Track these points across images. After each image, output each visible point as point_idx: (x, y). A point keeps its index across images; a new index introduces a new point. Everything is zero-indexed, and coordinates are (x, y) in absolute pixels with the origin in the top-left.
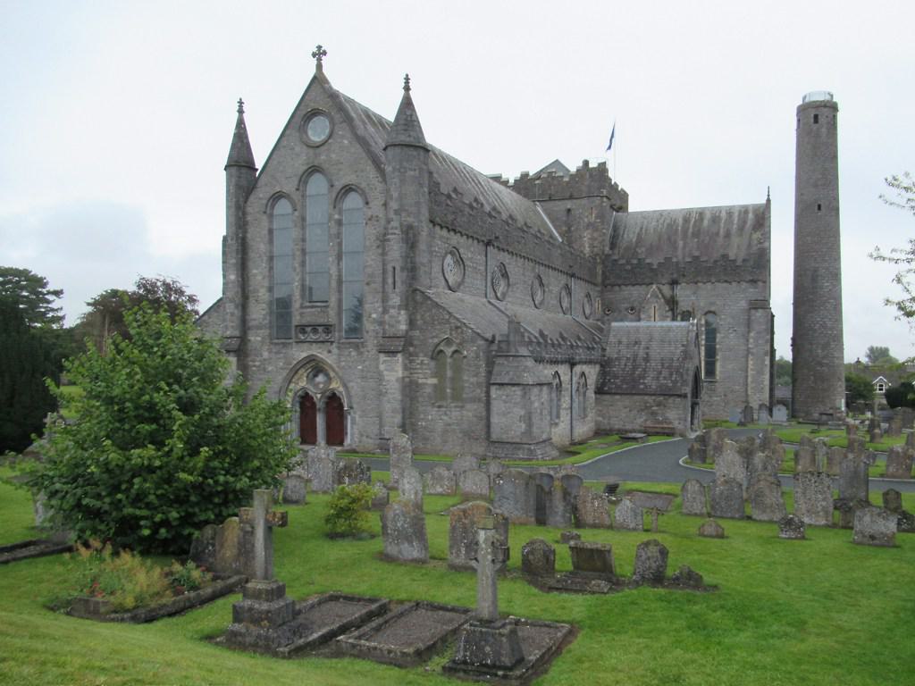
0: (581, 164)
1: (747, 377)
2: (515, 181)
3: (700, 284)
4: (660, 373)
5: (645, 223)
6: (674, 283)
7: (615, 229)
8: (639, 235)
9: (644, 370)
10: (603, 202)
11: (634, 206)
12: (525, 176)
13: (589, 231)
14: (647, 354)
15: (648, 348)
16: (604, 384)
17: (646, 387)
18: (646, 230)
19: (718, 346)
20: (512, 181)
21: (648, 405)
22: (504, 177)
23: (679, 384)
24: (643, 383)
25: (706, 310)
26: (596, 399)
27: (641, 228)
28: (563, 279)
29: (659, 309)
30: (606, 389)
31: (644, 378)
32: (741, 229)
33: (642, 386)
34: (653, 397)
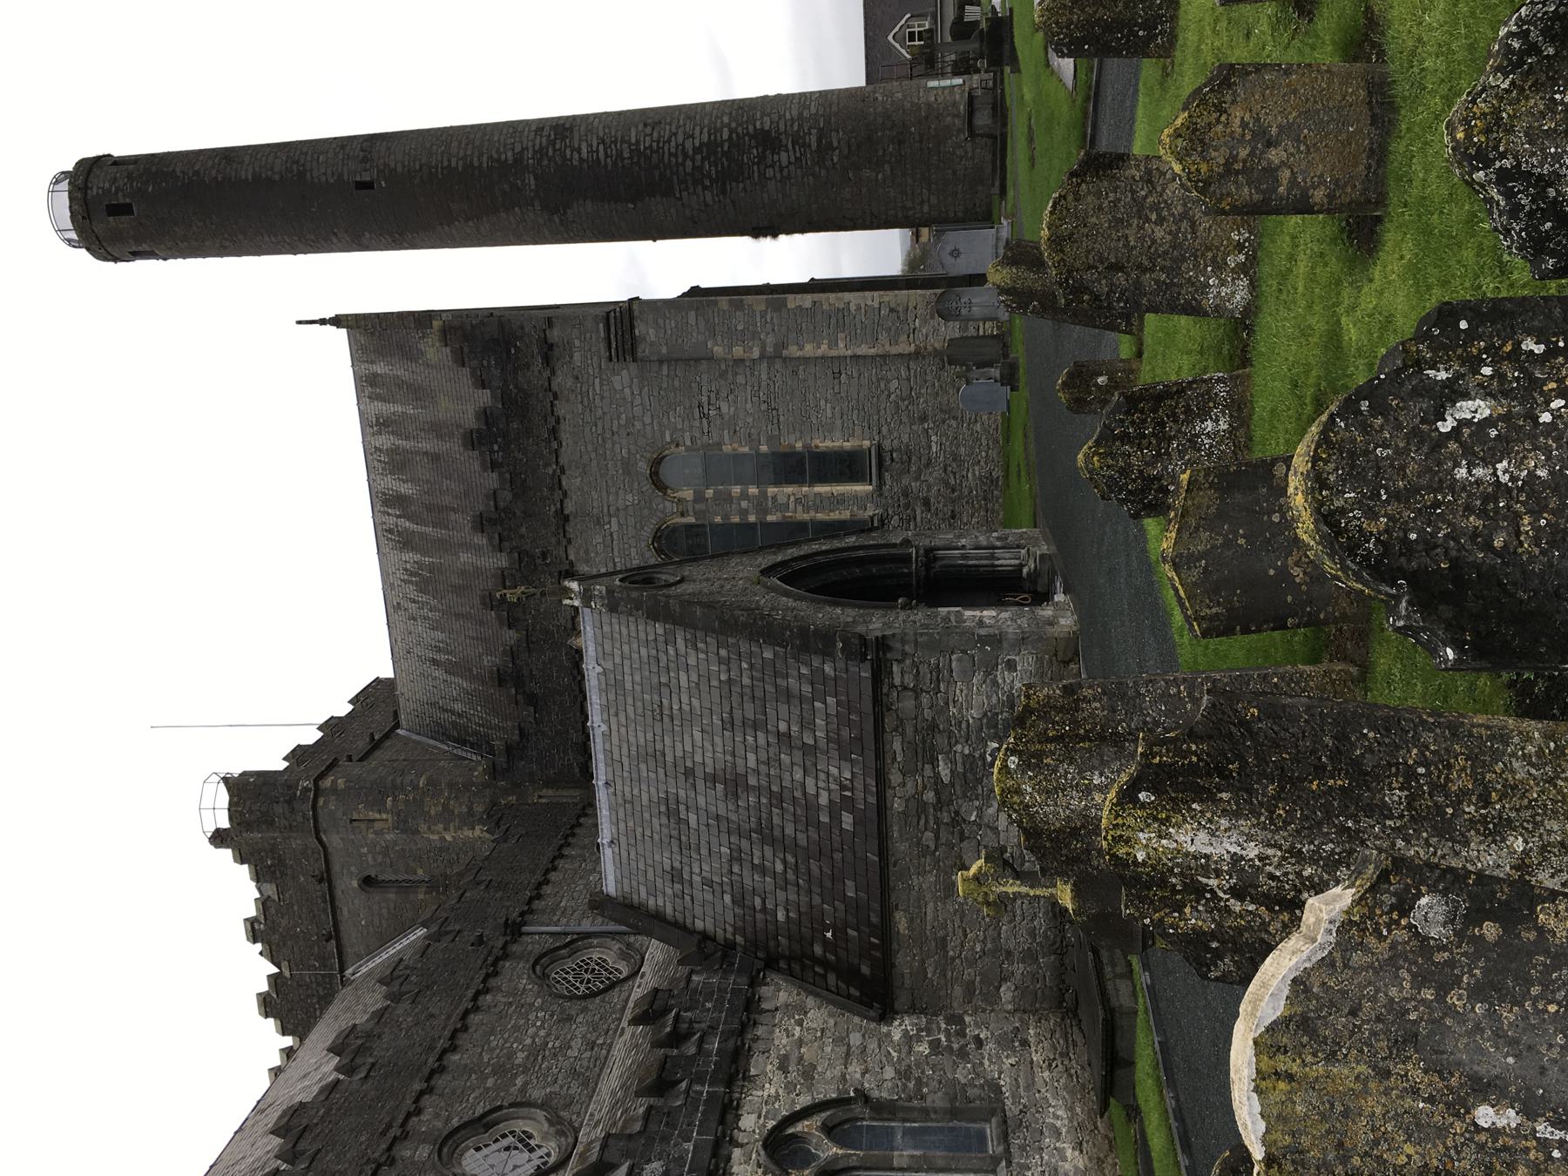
0: (227, 854)
2: (284, 1032)
3: (570, 507)
4: (784, 739)
5: (417, 650)
7: (441, 732)
8: (451, 669)
9: (778, 799)
10: (334, 789)
11: (387, 672)
12: (268, 1005)
13: (423, 827)
14: (712, 779)
15: (689, 773)
16: (849, 974)
17: (848, 804)
18: (439, 650)
19: (764, 448)
20: (288, 1041)
21: (930, 796)
22: (276, 1061)
23: (828, 669)
24: (834, 811)
25: (647, 487)
26: (913, 1009)
27: (434, 662)
28: (516, 976)
30: (865, 970)
31: (811, 805)
32: (417, 393)
33: (847, 820)
34: (895, 778)
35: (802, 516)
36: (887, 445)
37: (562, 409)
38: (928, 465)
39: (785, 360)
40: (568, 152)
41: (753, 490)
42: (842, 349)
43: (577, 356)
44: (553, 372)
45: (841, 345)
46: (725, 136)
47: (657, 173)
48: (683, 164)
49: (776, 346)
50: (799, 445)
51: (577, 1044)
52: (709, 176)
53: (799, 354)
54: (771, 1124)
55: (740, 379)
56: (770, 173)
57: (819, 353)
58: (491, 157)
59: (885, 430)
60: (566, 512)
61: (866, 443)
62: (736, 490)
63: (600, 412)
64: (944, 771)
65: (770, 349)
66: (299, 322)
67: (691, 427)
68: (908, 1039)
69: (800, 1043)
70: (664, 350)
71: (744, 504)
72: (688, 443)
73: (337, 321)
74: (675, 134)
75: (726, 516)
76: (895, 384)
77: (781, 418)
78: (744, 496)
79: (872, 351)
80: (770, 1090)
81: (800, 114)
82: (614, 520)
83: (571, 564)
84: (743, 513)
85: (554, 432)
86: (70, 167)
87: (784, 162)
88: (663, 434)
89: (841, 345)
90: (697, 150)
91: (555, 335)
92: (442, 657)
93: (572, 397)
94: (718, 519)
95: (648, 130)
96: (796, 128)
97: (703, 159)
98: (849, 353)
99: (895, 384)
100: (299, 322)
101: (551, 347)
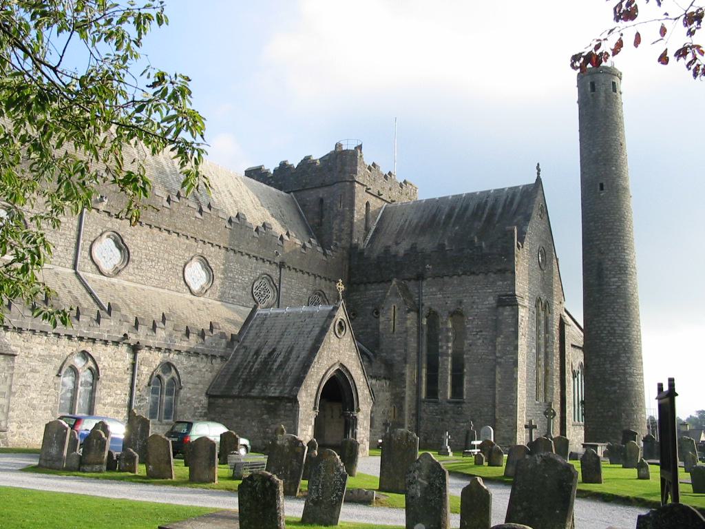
1: (495, 394)
3: (446, 279)
6: (420, 277)
12: (284, 166)
18: (410, 222)
25: (452, 309)
29: (399, 309)
35: (440, 370)
36: (464, 405)
37: (481, 277)
38: (456, 422)
39: (495, 367)
40: (613, 273)
41: (450, 351)
42: (498, 389)
43: (501, 283)
44: (495, 273)
45: (500, 389)
46: (619, 340)
47: (603, 311)
48: (607, 322)
49: (500, 362)
50: (465, 370)
51: (235, 293)
52: (602, 333)
53: (497, 372)
54: (174, 363)
55: (490, 348)
56: (602, 360)
57: (497, 380)
58: (612, 240)
59: (469, 405)
60: (445, 277)
61: (465, 397)
62: (450, 345)
63: (479, 291)
64: (265, 417)
65: (499, 360)
66: (538, 164)
67: (473, 328)
68: (200, 401)
69: (200, 371)
70: (500, 318)
71: (445, 348)
72: (468, 326)
73: (539, 180)
74: (620, 319)
75: (441, 340)
76: (486, 409)
77: (475, 364)
78: (448, 348)
79: (497, 401)
80: (185, 363)
81: (627, 373)
82: (441, 296)
83: (426, 279)
84: (442, 347)
85: (473, 273)
86: (615, 66)
87: (606, 366)
88: (471, 316)
89: (500, 389)
90: (612, 328)
91: (508, 274)
92: (407, 223)
93: (486, 281)
94: (440, 337)
95: (623, 307)
96: (621, 371)
97: (609, 331)
98: (497, 392)
99: (486, 409)
100: (538, 164)
101: (504, 273)
